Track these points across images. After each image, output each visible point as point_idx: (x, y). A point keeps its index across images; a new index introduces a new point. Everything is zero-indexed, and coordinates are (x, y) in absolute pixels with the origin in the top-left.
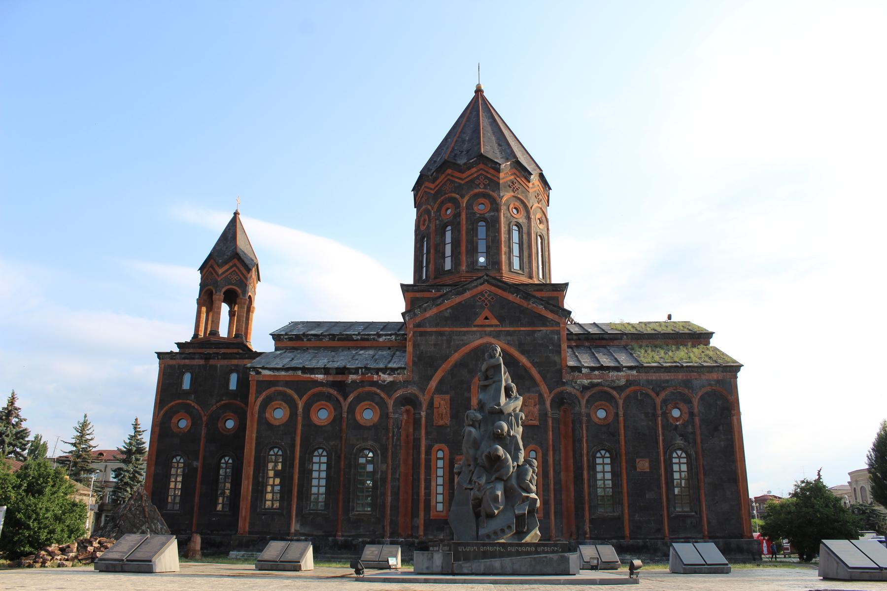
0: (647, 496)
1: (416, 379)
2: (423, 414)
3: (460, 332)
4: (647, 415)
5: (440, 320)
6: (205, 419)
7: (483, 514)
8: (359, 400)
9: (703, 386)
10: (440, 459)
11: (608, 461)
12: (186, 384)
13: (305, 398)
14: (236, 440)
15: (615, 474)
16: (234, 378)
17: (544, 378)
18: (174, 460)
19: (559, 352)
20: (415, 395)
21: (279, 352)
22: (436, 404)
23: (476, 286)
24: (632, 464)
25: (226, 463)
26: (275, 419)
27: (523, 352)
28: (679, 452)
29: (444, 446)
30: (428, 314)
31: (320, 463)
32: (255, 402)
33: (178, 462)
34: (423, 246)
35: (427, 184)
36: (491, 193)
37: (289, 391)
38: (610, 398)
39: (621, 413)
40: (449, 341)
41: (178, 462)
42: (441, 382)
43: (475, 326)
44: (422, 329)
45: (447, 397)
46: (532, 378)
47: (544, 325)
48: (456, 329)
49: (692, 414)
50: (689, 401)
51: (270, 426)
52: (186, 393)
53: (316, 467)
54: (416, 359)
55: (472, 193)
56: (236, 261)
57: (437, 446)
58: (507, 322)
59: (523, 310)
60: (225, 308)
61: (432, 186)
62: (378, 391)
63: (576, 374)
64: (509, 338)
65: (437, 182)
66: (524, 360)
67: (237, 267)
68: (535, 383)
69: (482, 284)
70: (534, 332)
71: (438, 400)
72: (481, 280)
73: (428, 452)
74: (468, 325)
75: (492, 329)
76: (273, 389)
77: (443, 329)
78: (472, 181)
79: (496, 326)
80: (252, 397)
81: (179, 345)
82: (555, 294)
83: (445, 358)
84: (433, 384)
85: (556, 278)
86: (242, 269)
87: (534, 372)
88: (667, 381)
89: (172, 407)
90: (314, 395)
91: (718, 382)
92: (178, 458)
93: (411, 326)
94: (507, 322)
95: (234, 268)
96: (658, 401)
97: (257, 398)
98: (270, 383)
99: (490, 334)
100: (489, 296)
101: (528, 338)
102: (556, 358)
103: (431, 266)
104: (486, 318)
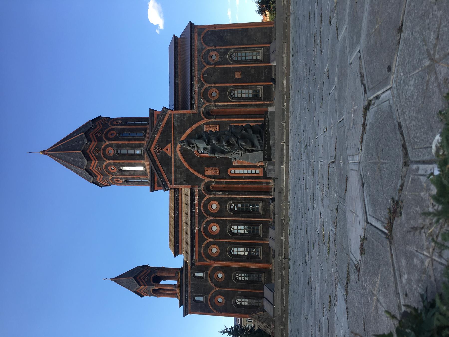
1: (197, 183)
2: (213, 180)
5: (168, 172)
6: (217, 289)
7: (252, 148)
9: (201, 43)
10: (235, 172)
11: (236, 92)
12: (201, 299)
13: (206, 237)
14: (227, 271)
15: (243, 88)
16: (198, 274)
17: (197, 122)
18: (238, 303)
19: (184, 114)
20: (205, 184)
21: (184, 252)
22: (209, 174)
24: (238, 81)
25: (239, 276)
26: (217, 252)
28: (233, 57)
29: (229, 171)
30: (166, 178)
31: (237, 229)
32: (208, 262)
33: (239, 301)
34: (131, 182)
35: (98, 180)
36: (103, 146)
37: (204, 245)
38: (207, 90)
39: (213, 85)
40: (179, 168)
41: (239, 301)
42: (198, 171)
43: (171, 155)
44: (173, 181)
45: (206, 169)
46: (197, 128)
49: (214, 50)
50: (208, 51)
51: (220, 254)
52: (206, 298)
53: (239, 231)
54: (188, 184)
55: (102, 157)
56: (138, 278)
57: (229, 173)
58: (169, 139)
60: (162, 282)
61: (99, 177)
62: (203, 202)
64: (177, 138)
65: (97, 174)
66: (188, 132)
67: (141, 277)
68: (200, 126)
69: (151, 152)
70: (174, 126)
71: (206, 173)
73: (232, 178)
75: (173, 147)
76: (202, 254)
79: (171, 144)
80: (206, 264)
81: (180, 305)
82: (155, 116)
83: (187, 169)
85: (147, 115)
86: (142, 274)
87: (194, 127)
88: (198, 61)
89: (212, 306)
90: (205, 233)
91: (199, 35)
92: (237, 301)
93: (171, 186)
94: (169, 139)
95: (142, 278)
96: (208, 67)
97: (207, 262)
99: (175, 148)
100: (156, 148)
101: (177, 129)
102: (187, 116)
103: (141, 177)
104: (167, 149)
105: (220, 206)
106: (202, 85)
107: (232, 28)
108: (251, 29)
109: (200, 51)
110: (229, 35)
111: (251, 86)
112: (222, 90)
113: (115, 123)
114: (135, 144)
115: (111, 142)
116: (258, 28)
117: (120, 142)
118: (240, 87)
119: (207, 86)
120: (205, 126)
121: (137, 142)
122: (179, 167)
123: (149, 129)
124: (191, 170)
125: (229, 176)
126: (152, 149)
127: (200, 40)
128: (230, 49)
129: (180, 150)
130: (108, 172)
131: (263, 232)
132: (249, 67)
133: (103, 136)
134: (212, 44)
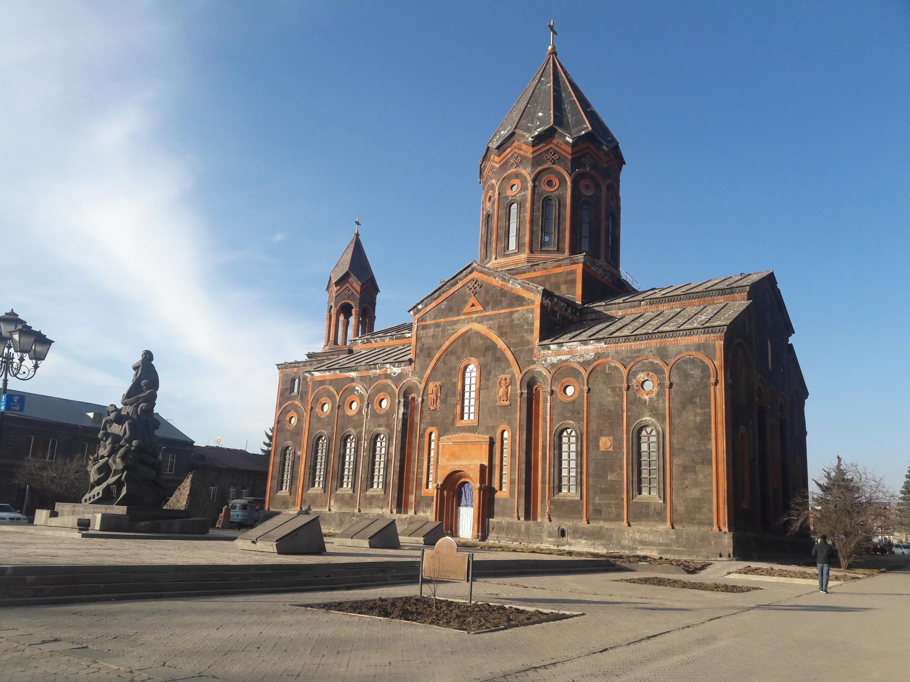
0: (610, 477)
2: (420, 399)
3: (452, 321)
4: (613, 390)
8: (378, 390)
19: (532, 331)
22: (430, 391)
23: (466, 276)
27: (502, 335)
30: (428, 308)
39: (586, 388)
40: (443, 332)
43: (464, 314)
44: (423, 323)
46: (507, 360)
47: (522, 305)
48: (448, 319)
49: (661, 385)
59: (503, 293)
62: (389, 382)
63: (546, 352)
64: (491, 322)
66: (501, 344)
68: (509, 366)
69: (471, 273)
70: (512, 313)
72: (470, 269)
74: (458, 314)
77: (439, 321)
78: (506, 163)
84: (428, 372)
88: (639, 351)
95: (347, 285)
98: (322, 382)
102: (529, 338)
104: (473, 305)
105: (382, 416)
106: (585, 364)
107: (713, 426)
108: (711, 474)
109: (662, 353)
110: (698, 418)
111: (581, 473)
112: (572, 409)
113: (582, 183)
114: (525, 234)
115: (530, 185)
116: (711, 491)
117: (528, 205)
118: (579, 449)
119: (585, 375)
120: (508, 376)
121: (527, 239)
122: (444, 331)
123: (561, 256)
124: (438, 355)
125: (425, 430)
126: (475, 275)
127: (687, 350)
128: (663, 421)
129: (470, 330)
130: (487, 192)
131: (343, 495)
132: (621, 468)
133: (546, 166)
134: (675, 379)
